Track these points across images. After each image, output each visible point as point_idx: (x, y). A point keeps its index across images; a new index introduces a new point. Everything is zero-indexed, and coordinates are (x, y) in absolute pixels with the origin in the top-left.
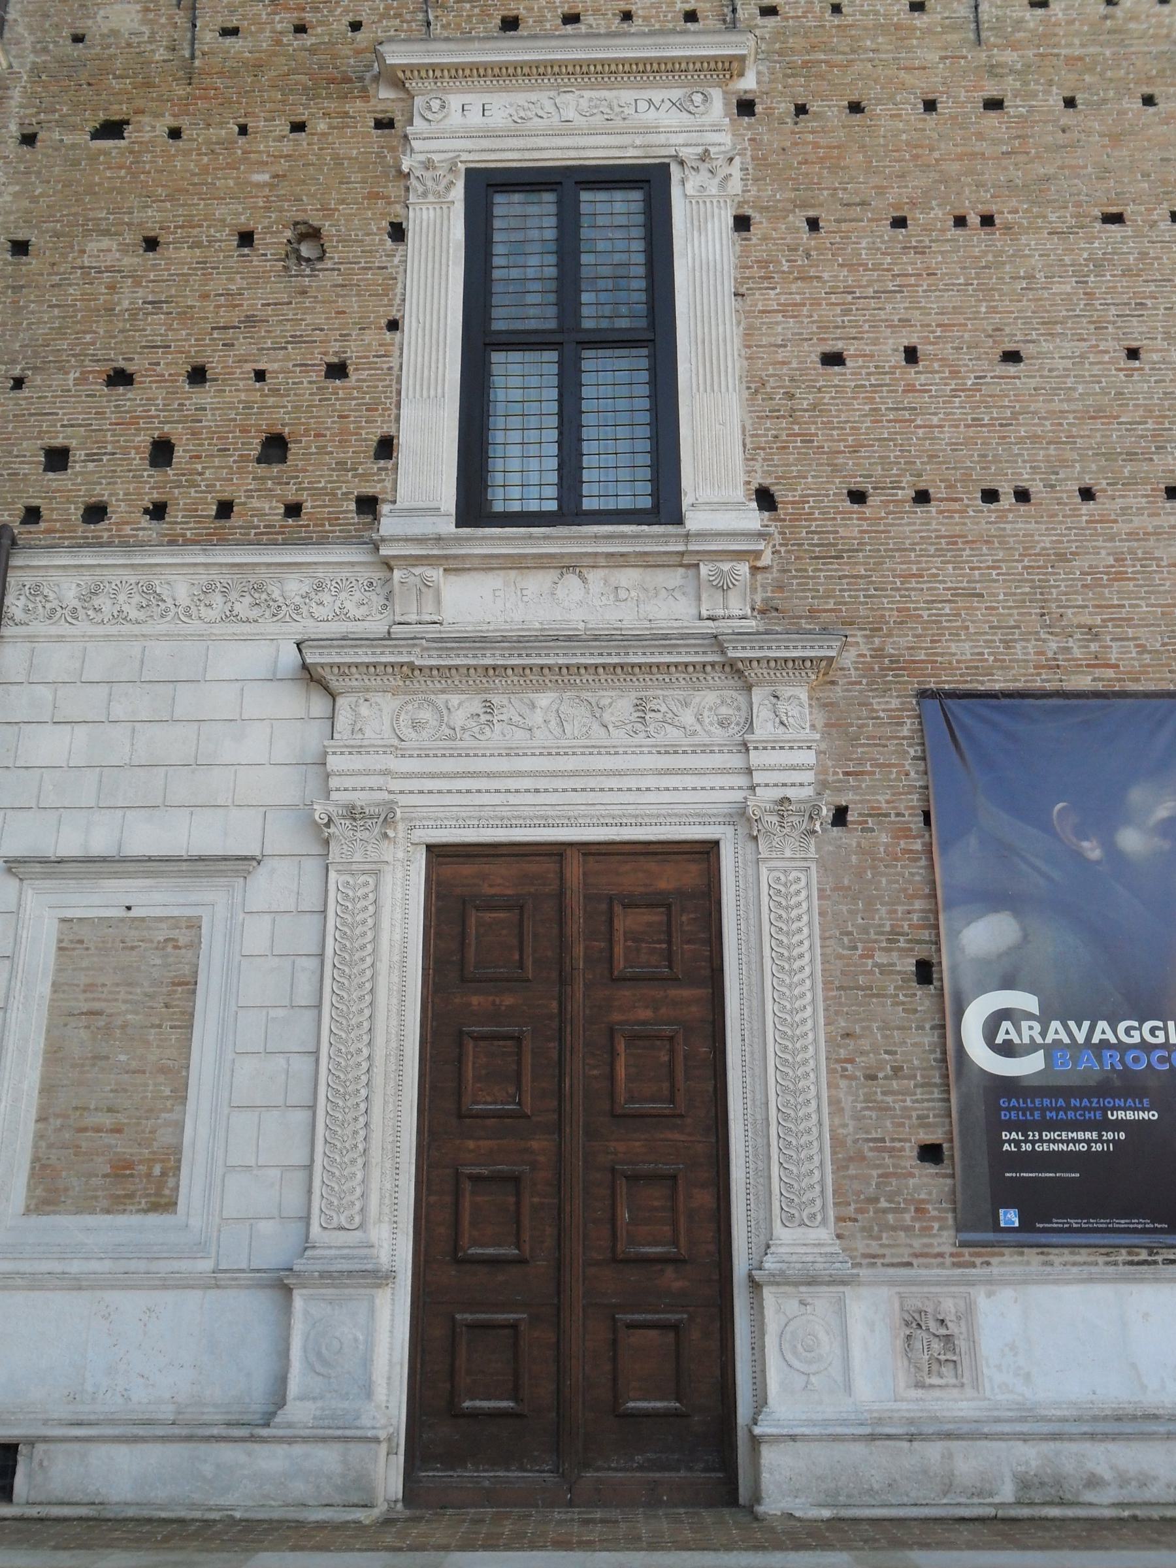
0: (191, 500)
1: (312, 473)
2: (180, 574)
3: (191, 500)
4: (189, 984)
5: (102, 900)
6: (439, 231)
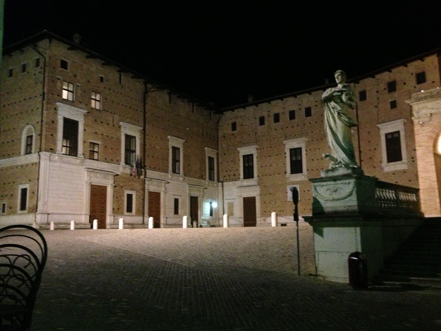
0: (231, 179)
1: (236, 177)
2: (231, 183)
3: (231, 179)
4: (233, 205)
5: (230, 201)
6: (241, 159)
